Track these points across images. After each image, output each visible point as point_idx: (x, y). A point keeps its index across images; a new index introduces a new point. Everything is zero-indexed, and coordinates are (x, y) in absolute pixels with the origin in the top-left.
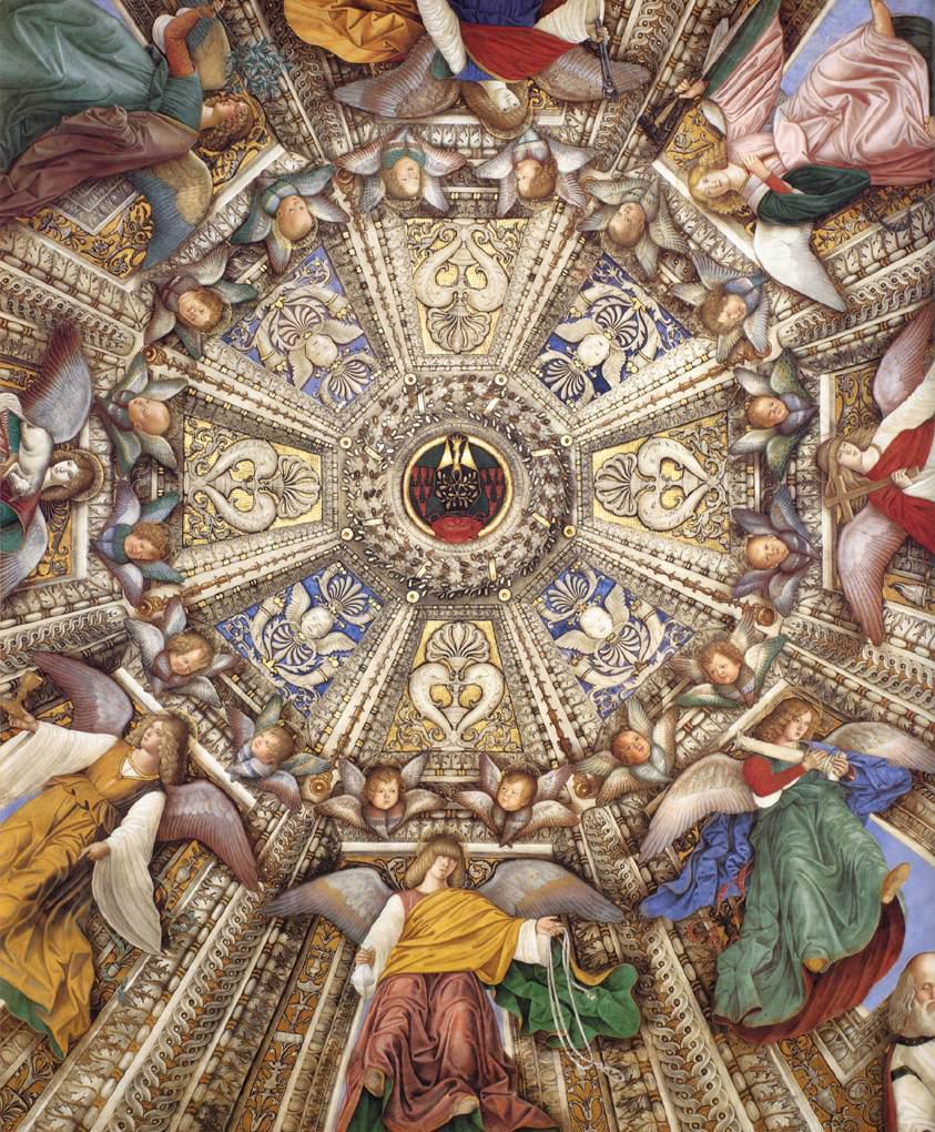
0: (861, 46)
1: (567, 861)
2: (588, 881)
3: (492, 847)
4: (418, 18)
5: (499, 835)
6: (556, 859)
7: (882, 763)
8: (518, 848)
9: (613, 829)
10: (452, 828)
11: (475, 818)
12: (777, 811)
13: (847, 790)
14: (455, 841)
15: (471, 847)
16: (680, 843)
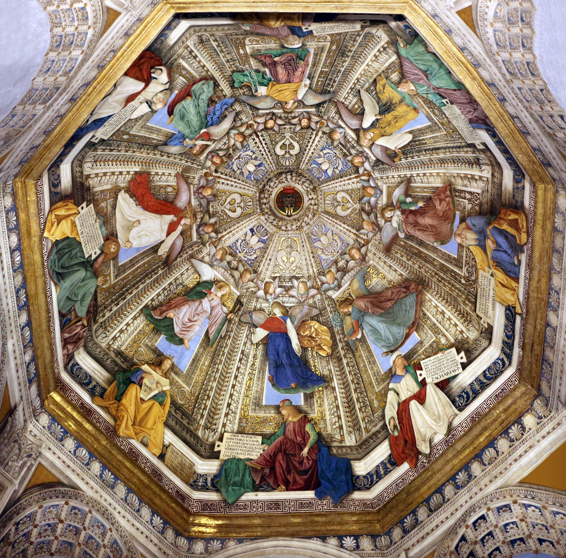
0: (191, 335)
1: (254, 108)
2: (248, 104)
3: (275, 111)
4: (298, 334)
5: (273, 114)
6: (258, 109)
7: (175, 145)
8: (268, 111)
9: (243, 117)
10: (286, 115)
11: (280, 118)
12: (201, 129)
13: (184, 137)
14: (285, 112)
15: (281, 111)
16: (225, 116)
